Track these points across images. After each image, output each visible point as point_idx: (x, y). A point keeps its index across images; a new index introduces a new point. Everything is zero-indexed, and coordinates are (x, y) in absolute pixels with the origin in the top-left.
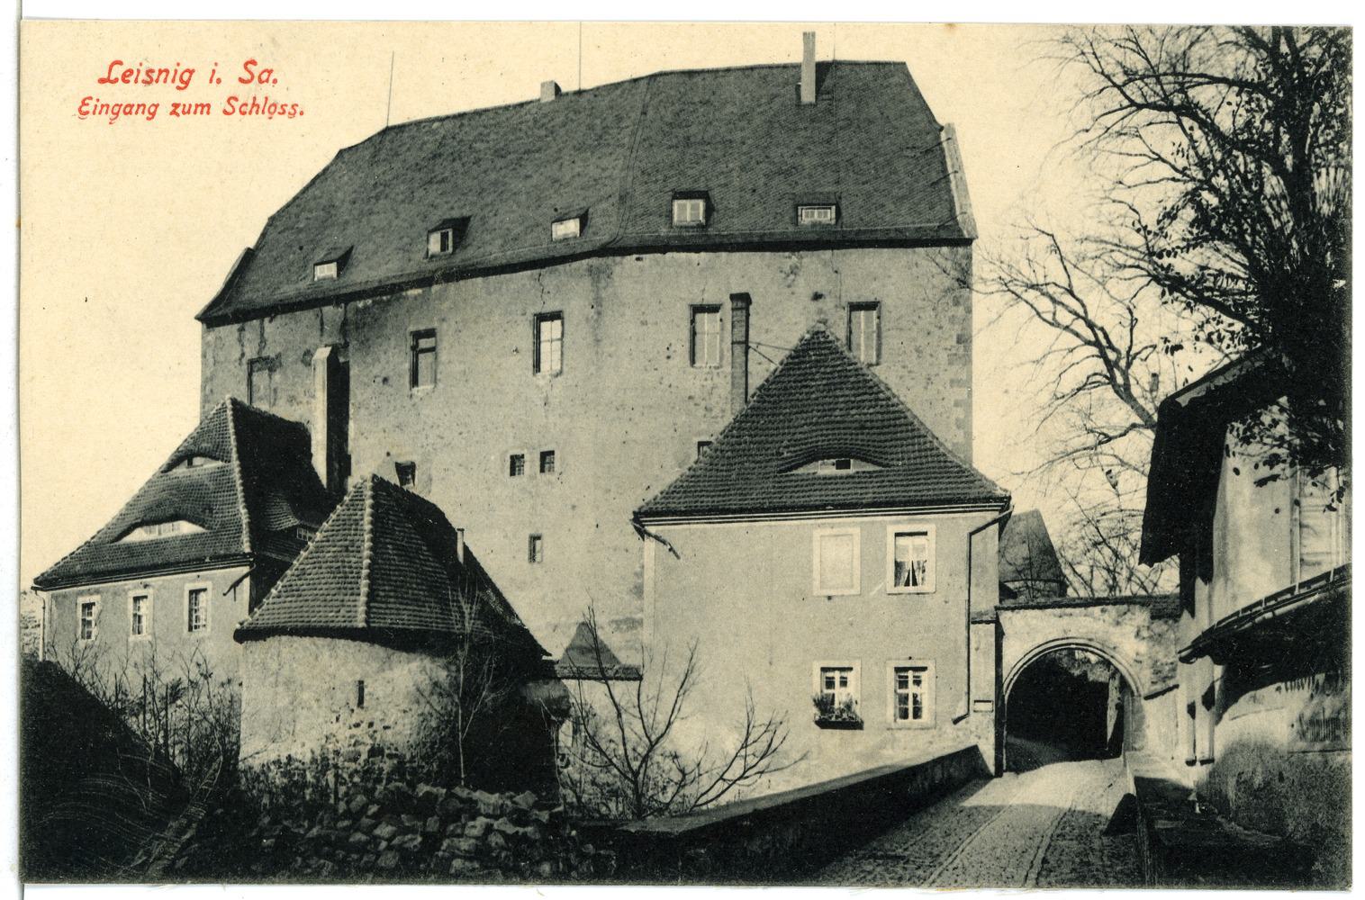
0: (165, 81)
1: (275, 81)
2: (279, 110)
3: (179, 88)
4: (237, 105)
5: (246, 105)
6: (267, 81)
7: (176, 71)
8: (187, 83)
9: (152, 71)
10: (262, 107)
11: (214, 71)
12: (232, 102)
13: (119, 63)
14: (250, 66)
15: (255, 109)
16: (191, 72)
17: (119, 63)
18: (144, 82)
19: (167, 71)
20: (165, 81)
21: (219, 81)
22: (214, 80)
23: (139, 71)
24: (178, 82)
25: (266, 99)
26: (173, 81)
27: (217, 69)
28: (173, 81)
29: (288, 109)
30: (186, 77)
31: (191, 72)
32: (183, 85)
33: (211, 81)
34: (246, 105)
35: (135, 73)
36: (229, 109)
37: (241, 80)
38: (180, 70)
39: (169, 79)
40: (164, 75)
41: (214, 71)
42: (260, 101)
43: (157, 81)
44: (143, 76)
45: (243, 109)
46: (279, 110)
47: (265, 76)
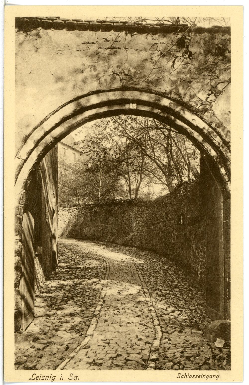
2: (192, 377)
4: (181, 375)
12: (179, 374)
13: (35, 374)
14: (71, 375)
17: (35, 374)
19: (48, 376)
21: (63, 379)
24: (51, 380)
29: (195, 377)
30: (53, 379)
36: (179, 377)
37: (69, 379)
38: (52, 376)
42: (187, 374)
44: (42, 378)
45: (183, 377)
46: (192, 377)
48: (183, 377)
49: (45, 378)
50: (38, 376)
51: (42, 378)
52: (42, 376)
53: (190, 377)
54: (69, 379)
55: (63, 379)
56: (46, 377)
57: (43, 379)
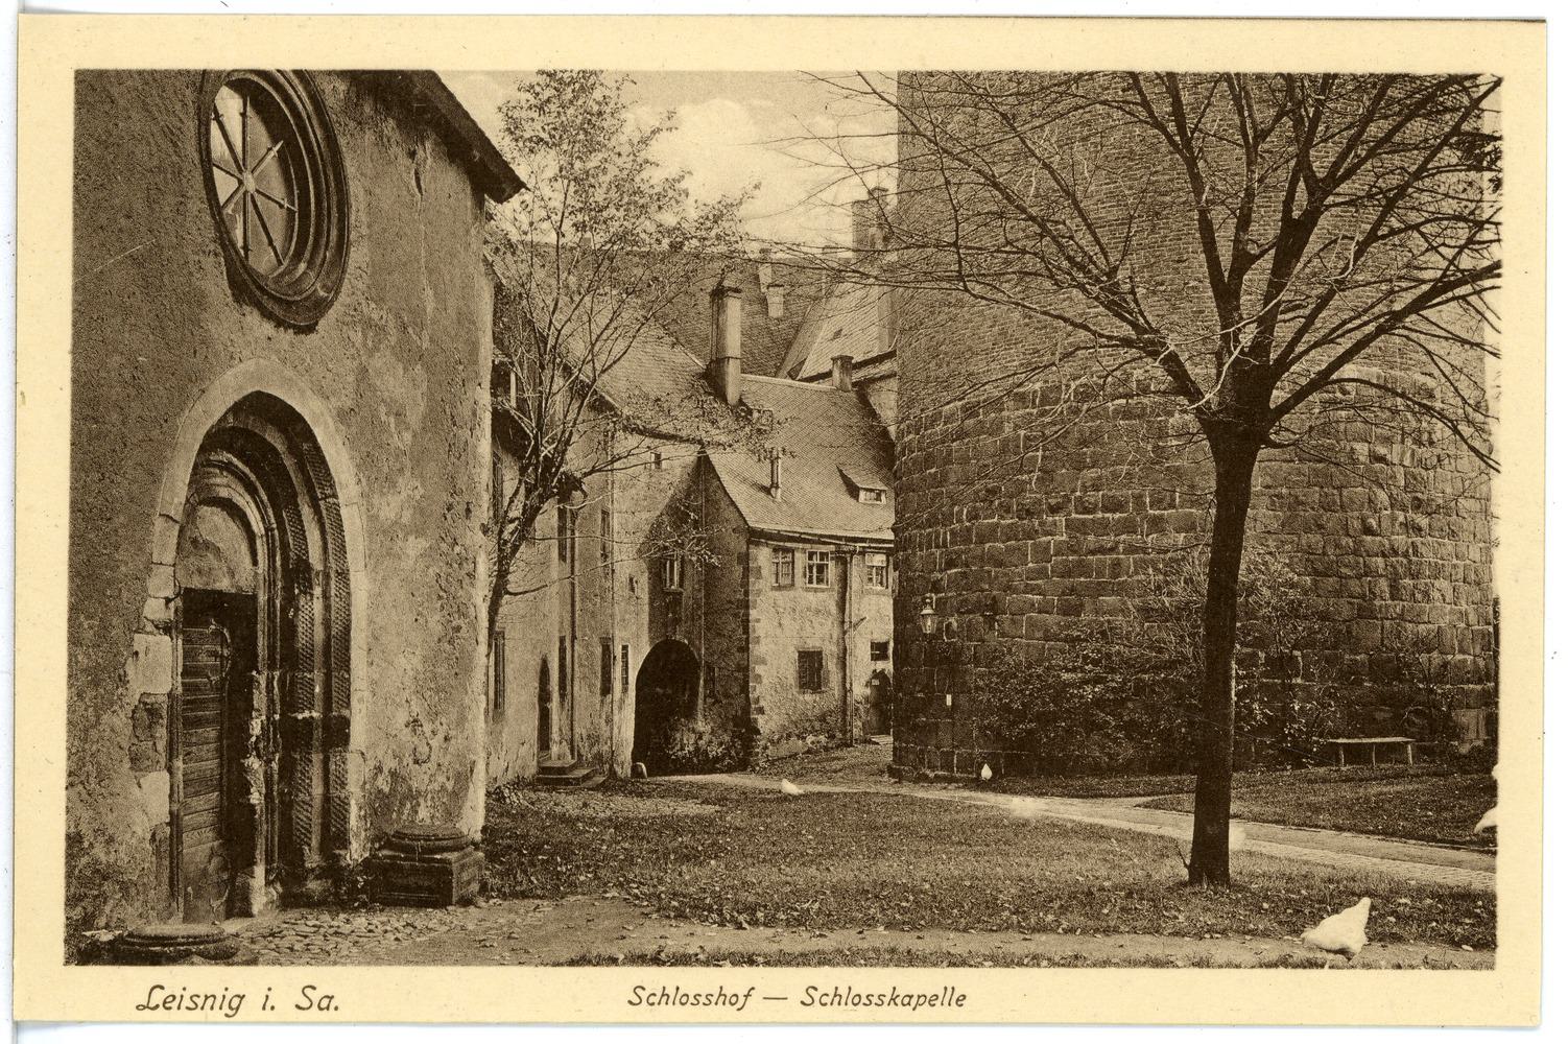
0: (212, 1008)
1: (336, 1008)
2: (864, 1000)
3: (227, 1015)
6: (328, 1008)
8: (238, 1008)
12: (811, 991)
13: (162, 988)
14: (308, 991)
15: (837, 998)
16: (242, 997)
17: (162, 988)
18: (188, 1008)
20: (212, 1008)
21: (273, 1008)
22: (268, 1007)
24: (226, 1009)
29: (875, 1000)
30: (234, 1005)
31: (242, 997)
32: (231, 1013)
33: (264, 1008)
36: (809, 1001)
37: (298, 1007)
38: (229, 996)
40: (210, 1000)
43: (202, 1008)
44: (187, 1002)
45: (825, 999)
46: (864, 1000)
47: (324, 1003)
48: (825, 999)
49: (200, 1001)
50: (174, 997)
51: (187, 1002)
53: (856, 1000)
54: (298, 1007)
55: (273, 1008)
56: (207, 997)
57: (193, 1006)
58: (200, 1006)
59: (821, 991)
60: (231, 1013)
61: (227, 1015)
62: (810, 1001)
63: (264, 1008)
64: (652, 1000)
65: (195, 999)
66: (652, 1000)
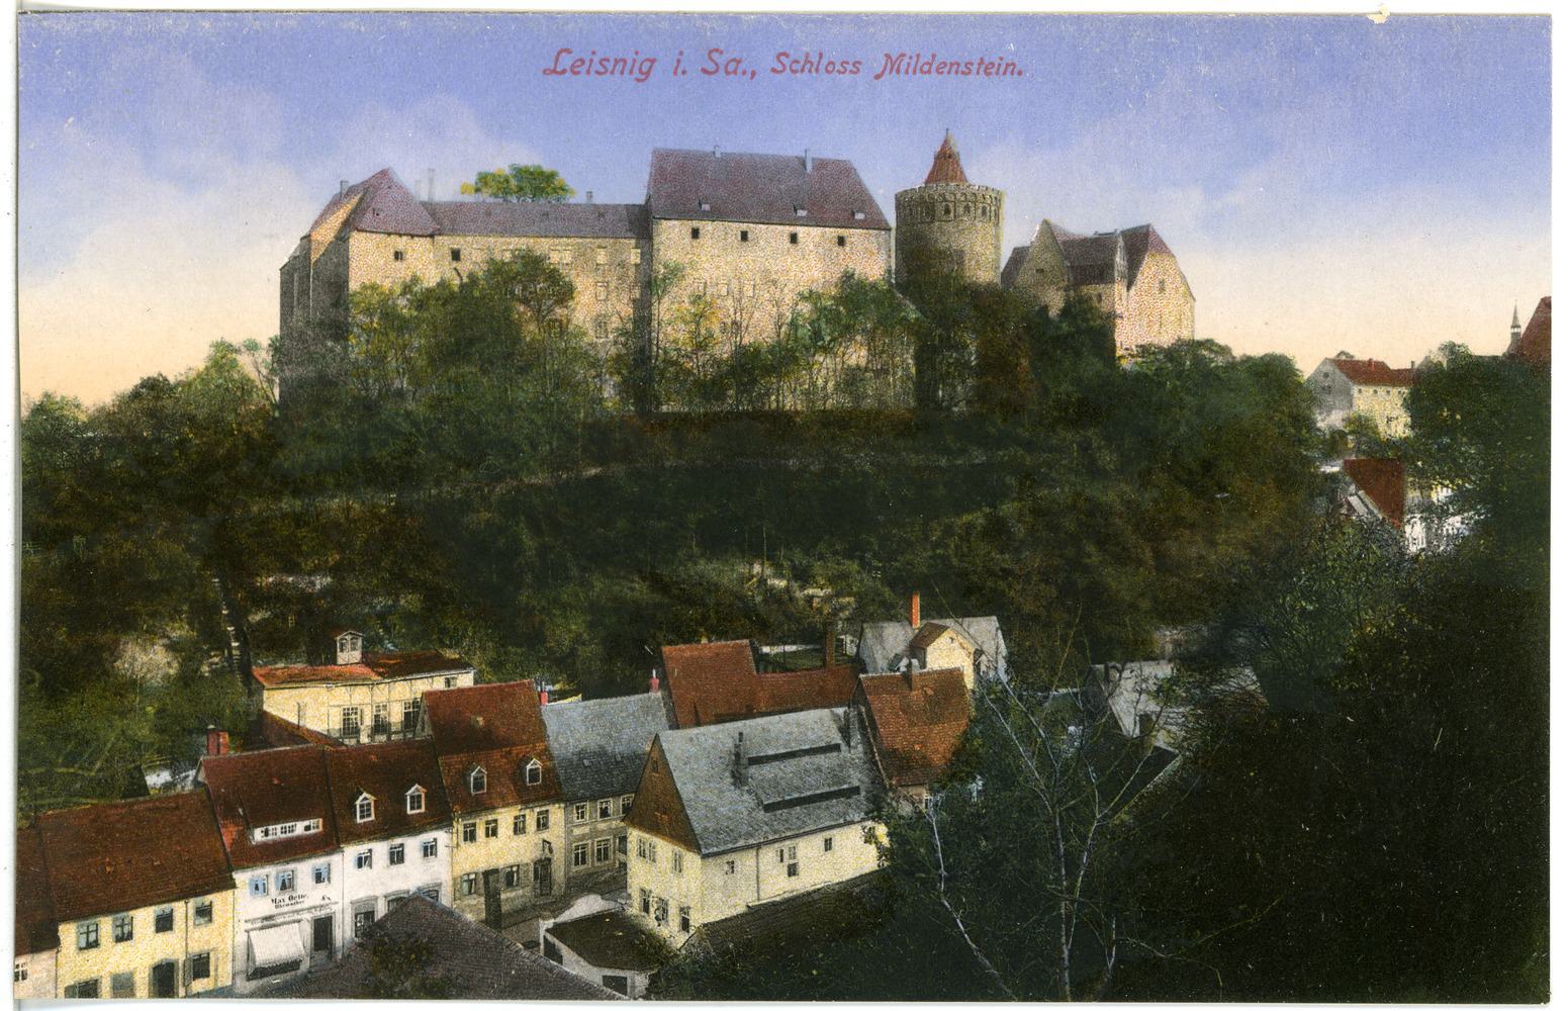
0: (622, 73)
3: (638, 80)
5: (797, 62)
6: (735, 72)
7: (634, 61)
8: (648, 73)
9: (608, 60)
10: (815, 66)
11: (679, 61)
12: (782, 58)
13: (568, 51)
14: (715, 56)
15: (808, 66)
16: (653, 61)
18: (598, 73)
19: (625, 61)
21: (684, 72)
22: (679, 71)
23: (591, 61)
24: (636, 74)
25: (821, 55)
26: (631, 72)
27: (683, 58)
28: (631, 72)
30: (645, 70)
31: (653, 61)
32: (643, 77)
33: (675, 73)
34: (797, 62)
35: (587, 63)
36: (780, 68)
37: (704, 71)
38: (639, 58)
39: (626, 71)
40: (621, 64)
41: (679, 61)
43: (612, 73)
44: (596, 66)
47: (732, 66)
50: (583, 61)
52: (596, 59)
55: (684, 72)
56: (616, 61)
58: (610, 68)
59: (791, 58)
60: (643, 77)
61: (638, 80)
62: (780, 68)
63: (675, 73)
64: (795, 67)
65: (604, 63)
66: (795, 67)
